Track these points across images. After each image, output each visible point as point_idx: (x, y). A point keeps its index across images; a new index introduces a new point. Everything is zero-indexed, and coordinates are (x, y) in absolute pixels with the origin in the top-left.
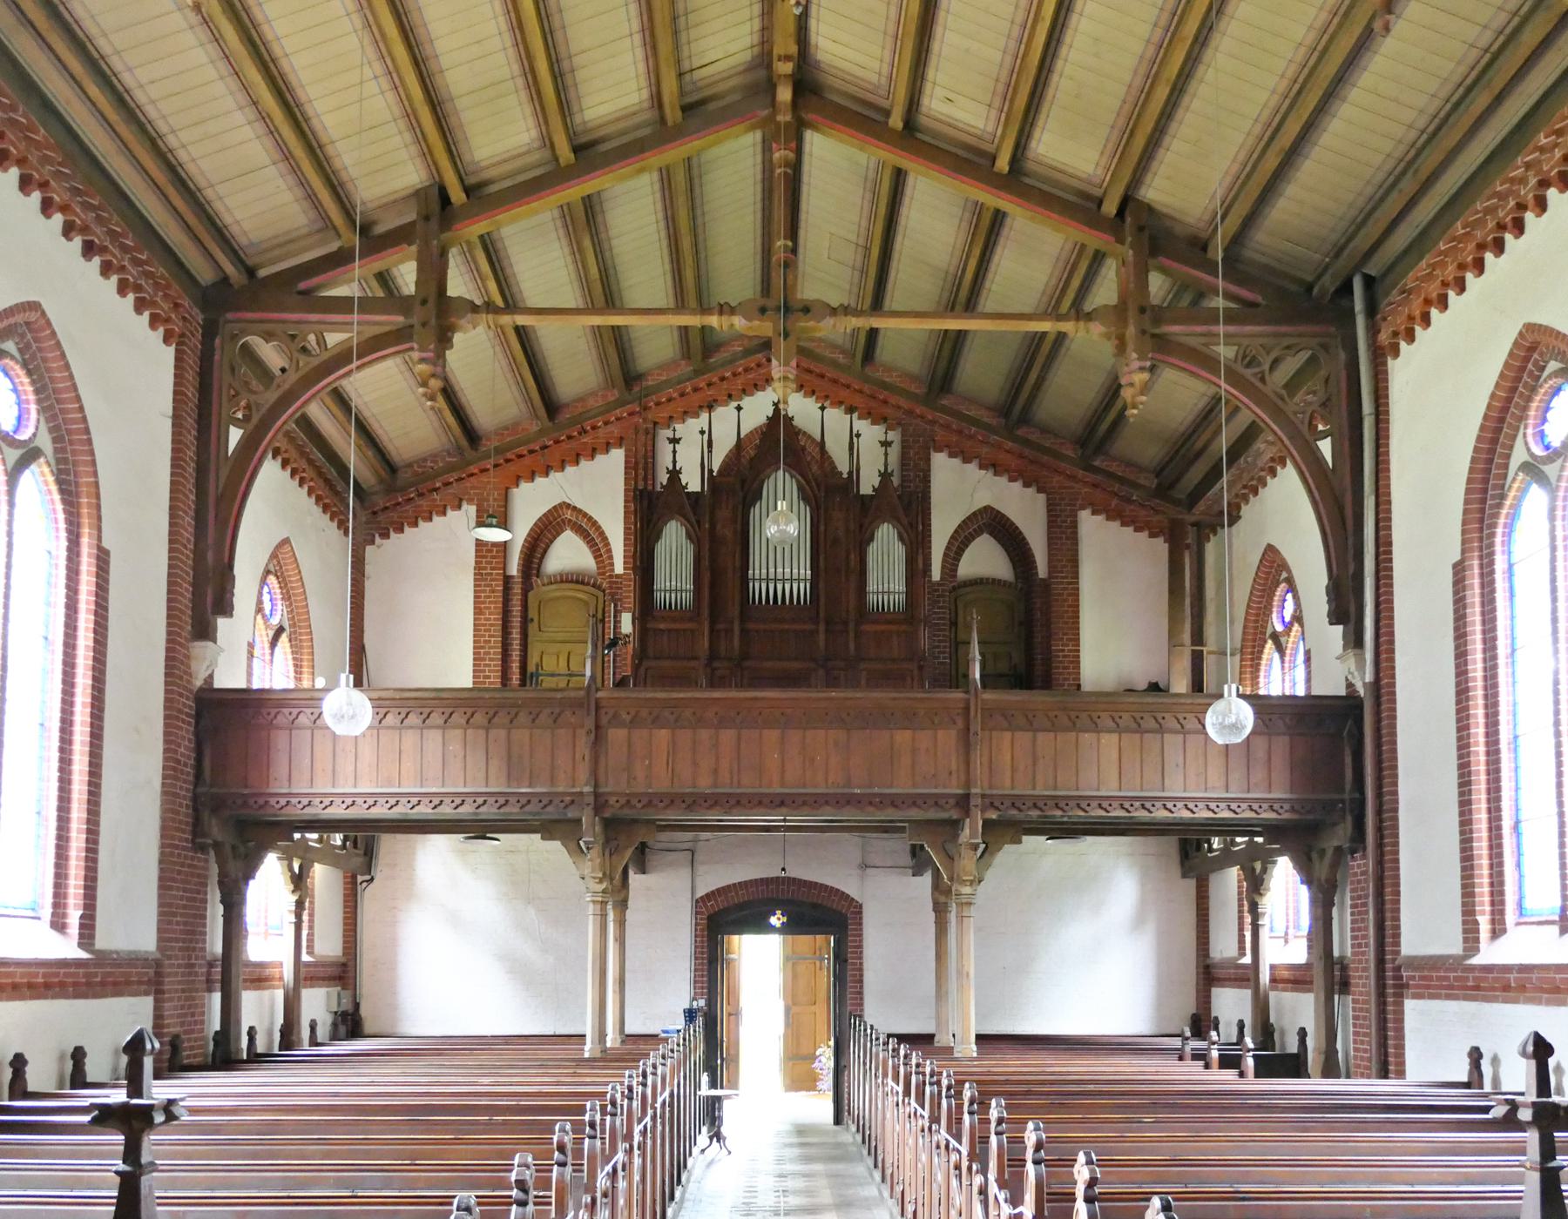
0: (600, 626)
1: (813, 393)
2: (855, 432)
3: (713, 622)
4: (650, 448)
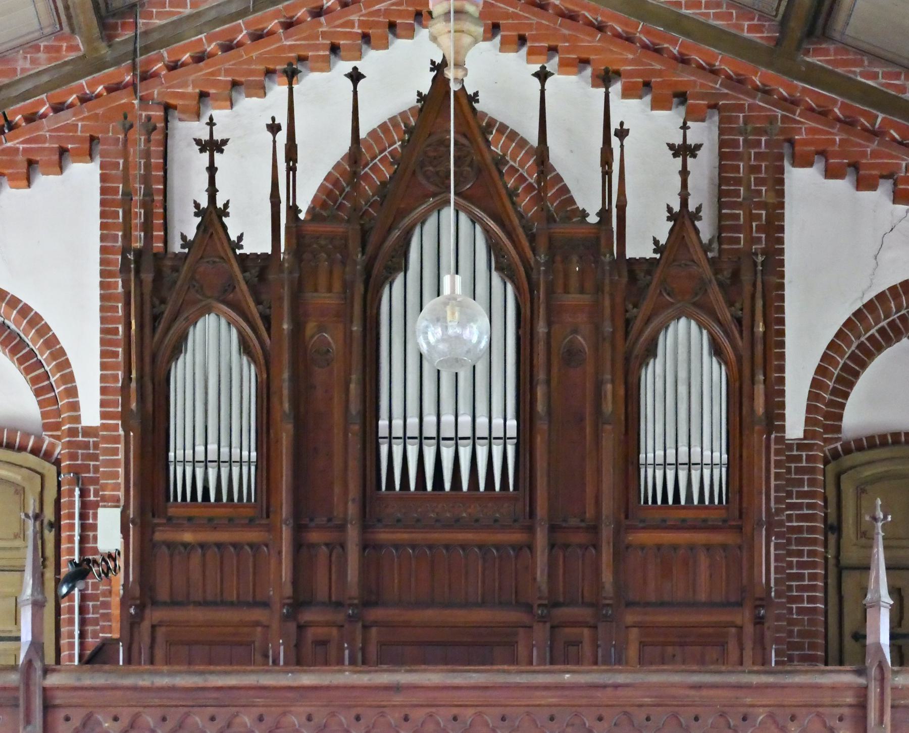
0: (50, 536)
1: (522, 40)
2: (614, 125)
3: (299, 529)
4: (156, 160)
